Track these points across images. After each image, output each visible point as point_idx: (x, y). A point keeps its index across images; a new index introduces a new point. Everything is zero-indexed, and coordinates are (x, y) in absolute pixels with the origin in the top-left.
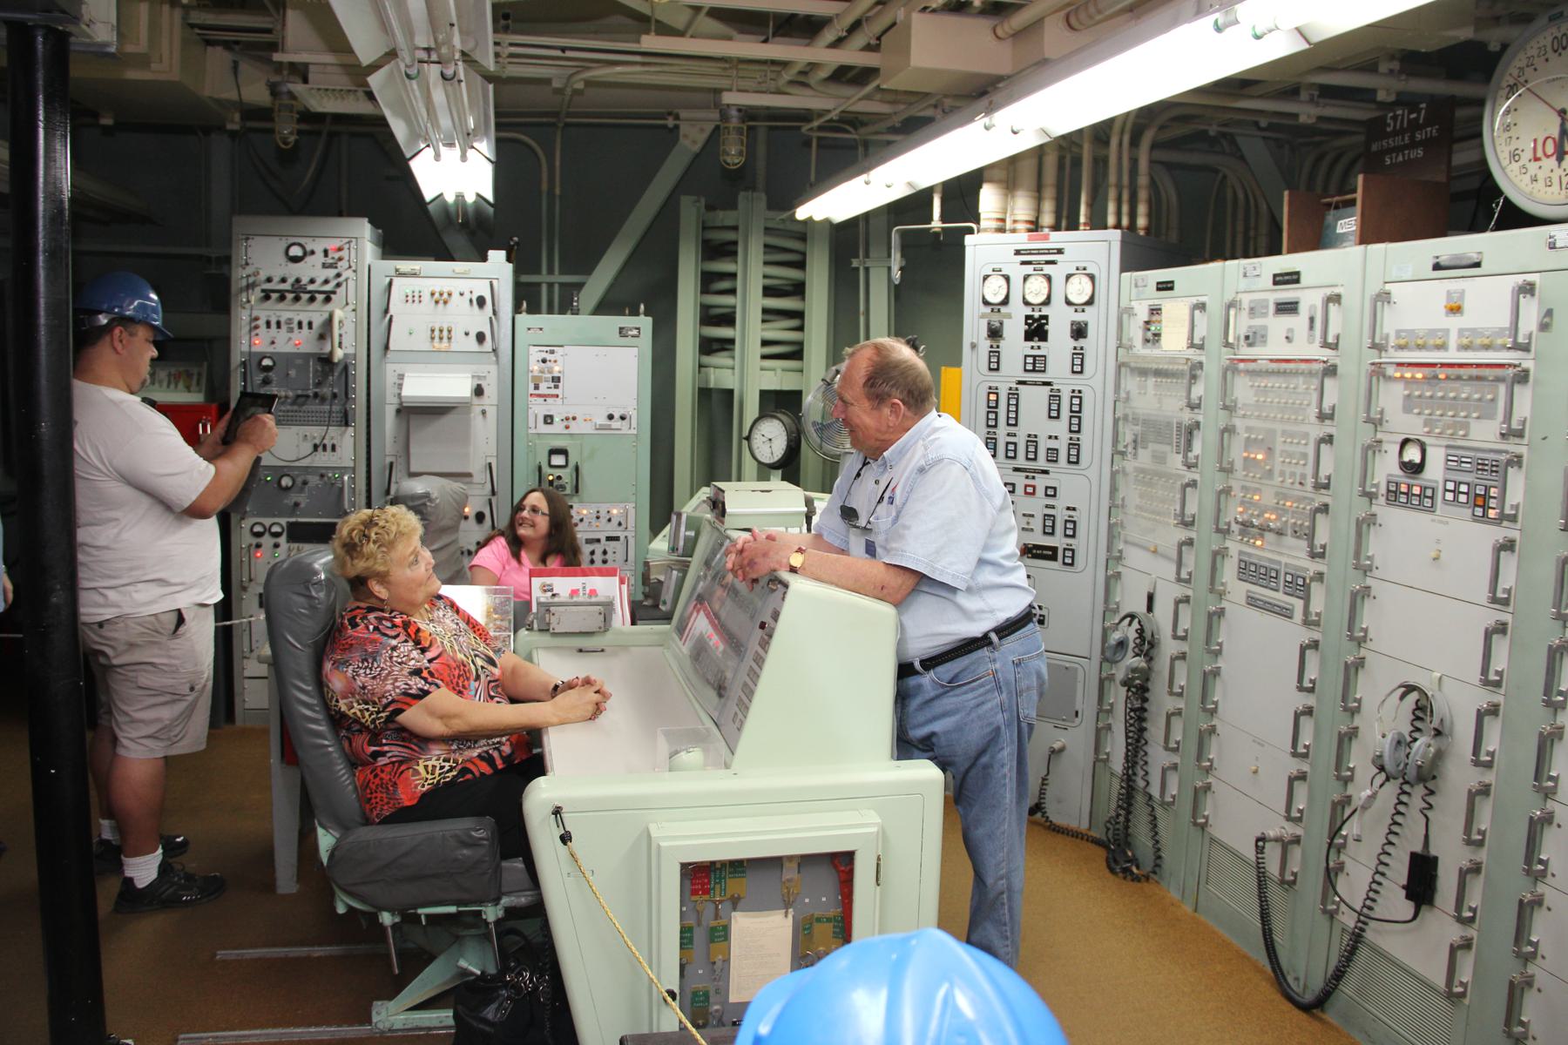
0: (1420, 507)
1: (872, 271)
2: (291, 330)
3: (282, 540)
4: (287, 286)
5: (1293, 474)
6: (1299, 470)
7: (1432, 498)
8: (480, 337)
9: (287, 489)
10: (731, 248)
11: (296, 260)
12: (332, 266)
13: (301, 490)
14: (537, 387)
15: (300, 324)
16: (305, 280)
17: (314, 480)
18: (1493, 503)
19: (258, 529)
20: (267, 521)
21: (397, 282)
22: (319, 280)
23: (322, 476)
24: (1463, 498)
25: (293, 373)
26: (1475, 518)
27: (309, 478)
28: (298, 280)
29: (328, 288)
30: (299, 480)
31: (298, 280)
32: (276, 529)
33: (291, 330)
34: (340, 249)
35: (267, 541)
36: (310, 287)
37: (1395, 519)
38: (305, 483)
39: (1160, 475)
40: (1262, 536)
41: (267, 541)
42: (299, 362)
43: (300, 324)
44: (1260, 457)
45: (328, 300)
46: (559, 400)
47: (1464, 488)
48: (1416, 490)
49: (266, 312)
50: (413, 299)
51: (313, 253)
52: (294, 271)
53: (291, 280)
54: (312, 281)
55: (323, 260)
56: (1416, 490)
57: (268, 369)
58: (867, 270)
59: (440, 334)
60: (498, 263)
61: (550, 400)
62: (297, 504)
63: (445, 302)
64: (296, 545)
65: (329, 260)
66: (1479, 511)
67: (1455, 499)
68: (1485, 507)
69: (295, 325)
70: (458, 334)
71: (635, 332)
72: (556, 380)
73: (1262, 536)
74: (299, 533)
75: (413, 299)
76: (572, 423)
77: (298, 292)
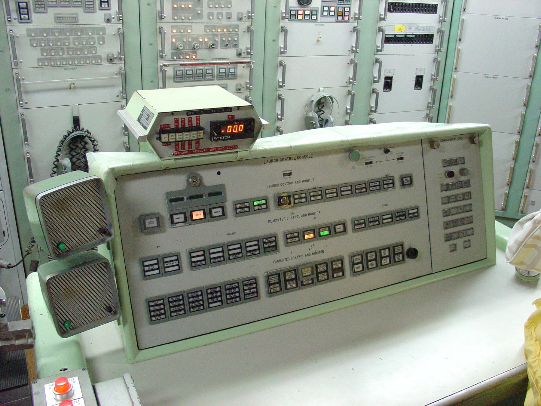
0: (311, 20)
5: (218, 14)
6: (225, 11)
7: (316, 15)
18: (347, 14)
24: (332, 13)
26: (337, 21)
37: (293, 27)
39: (74, 31)
40: (195, 53)
44: (190, 6)
47: (332, 9)
48: (307, 12)
56: (307, 12)
66: (340, 18)
67: (329, 14)
68: (343, 16)
73: (195, 53)
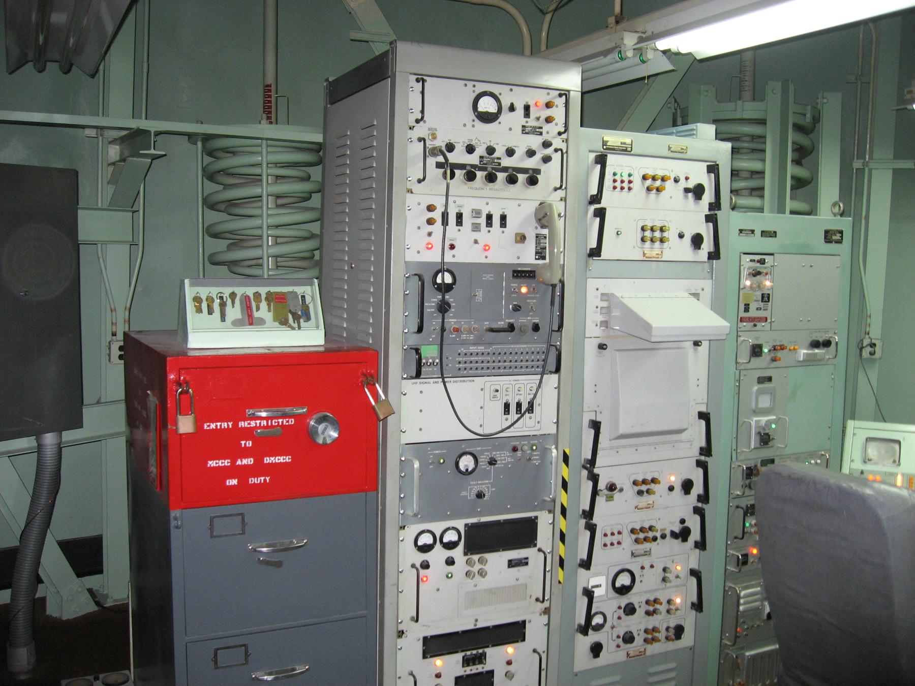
1: (874, 172)
2: (476, 228)
3: (458, 553)
4: (473, 159)
8: (697, 241)
9: (467, 473)
10: (763, 140)
11: (487, 118)
12: (537, 131)
13: (486, 475)
14: (747, 309)
15: (489, 217)
16: (500, 152)
17: (504, 457)
19: (426, 539)
20: (437, 527)
21: (611, 159)
22: (520, 152)
23: (515, 449)
25: (480, 294)
27: (497, 455)
28: (491, 150)
29: (531, 163)
30: (483, 459)
31: (491, 150)
32: (451, 537)
33: (476, 228)
34: (548, 105)
35: (438, 555)
36: (506, 162)
38: (492, 462)
41: (438, 555)
42: (488, 277)
43: (489, 217)
45: (533, 181)
46: (766, 325)
49: (471, 198)
50: (625, 185)
51: (512, 108)
52: (485, 135)
53: (480, 151)
54: (510, 152)
55: (523, 121)
57: (446, 288)
58: (870, 171)
59: (653, 234)
60: (705, 141)
61: (760, 325)
62: (480, 495)
63: (658, 190)
64: (476, 557)
65: (532, 122)
69: (483, 221)
70: (672, 235)
71: (838, 237)
72: (765, 298)
74: (481, 540)
75: (625, 185)
76: (779, 354)
77: (488, 170)
